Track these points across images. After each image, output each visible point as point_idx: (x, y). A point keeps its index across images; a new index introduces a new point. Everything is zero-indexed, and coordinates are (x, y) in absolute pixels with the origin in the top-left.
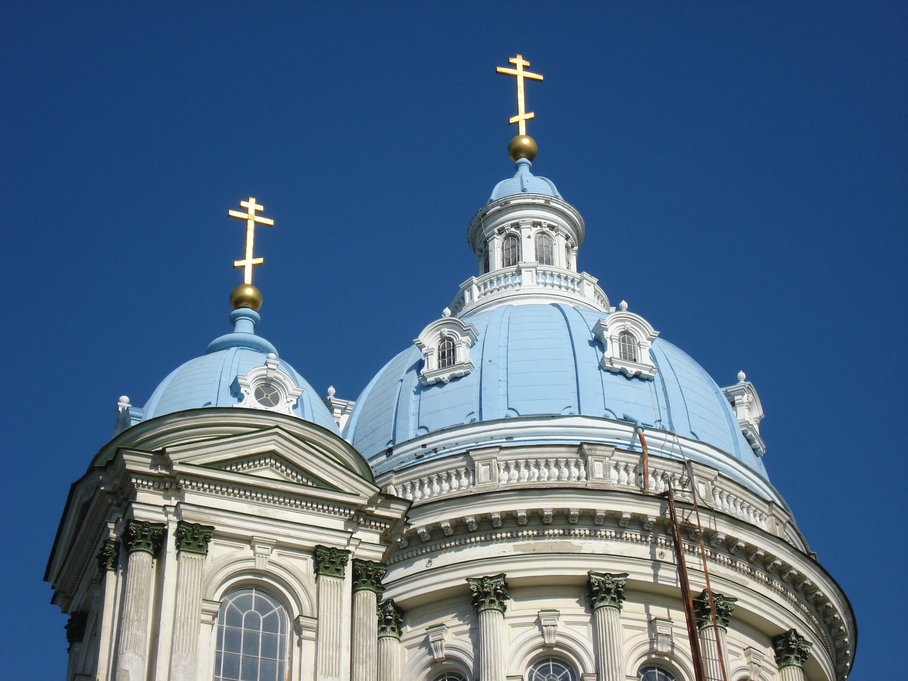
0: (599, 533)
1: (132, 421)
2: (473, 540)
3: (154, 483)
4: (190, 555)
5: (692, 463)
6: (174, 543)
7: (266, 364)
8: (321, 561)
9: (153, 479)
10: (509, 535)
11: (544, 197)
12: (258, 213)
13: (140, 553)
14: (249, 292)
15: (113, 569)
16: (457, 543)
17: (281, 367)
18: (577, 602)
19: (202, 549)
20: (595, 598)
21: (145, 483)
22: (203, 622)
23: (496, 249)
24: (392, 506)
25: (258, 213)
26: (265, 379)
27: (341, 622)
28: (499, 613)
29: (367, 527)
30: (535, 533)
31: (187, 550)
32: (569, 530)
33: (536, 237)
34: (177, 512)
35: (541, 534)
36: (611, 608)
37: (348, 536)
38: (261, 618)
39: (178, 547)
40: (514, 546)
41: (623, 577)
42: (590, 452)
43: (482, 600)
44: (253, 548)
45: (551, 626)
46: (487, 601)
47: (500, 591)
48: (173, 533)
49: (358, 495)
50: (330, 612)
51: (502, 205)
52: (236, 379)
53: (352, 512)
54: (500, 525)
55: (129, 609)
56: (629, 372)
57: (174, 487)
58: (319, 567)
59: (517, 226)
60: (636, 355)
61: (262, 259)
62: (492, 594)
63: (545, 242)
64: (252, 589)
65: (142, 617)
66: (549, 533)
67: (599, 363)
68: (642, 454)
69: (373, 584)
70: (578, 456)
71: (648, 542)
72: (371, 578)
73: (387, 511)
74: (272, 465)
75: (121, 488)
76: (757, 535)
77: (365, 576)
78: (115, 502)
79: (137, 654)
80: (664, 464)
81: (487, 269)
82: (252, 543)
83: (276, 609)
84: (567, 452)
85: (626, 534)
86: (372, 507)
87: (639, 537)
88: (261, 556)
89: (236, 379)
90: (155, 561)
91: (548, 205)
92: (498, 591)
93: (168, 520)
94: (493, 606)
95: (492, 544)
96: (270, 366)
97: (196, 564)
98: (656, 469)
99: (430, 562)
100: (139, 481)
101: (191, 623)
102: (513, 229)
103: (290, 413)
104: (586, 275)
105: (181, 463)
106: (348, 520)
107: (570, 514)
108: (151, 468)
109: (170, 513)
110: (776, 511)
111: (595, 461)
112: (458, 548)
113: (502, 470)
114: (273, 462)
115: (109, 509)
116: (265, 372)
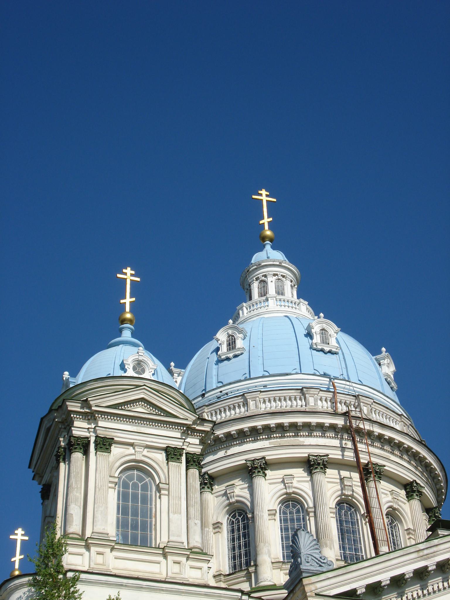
0: (313, 434)
1: (70, 384)
2: (248, 440)
3: (82, 416)
4: (102, 453)
5: (360, 396)
6: (94, 447)
7: (138, 353)
8: (169, 454)
9: (83, 414)
10: (266, 437)
11: (279, 261)
12: (132, 275)
13: (77, 453)
14: (128, 316)
15: (63, 461)
16: (240, 442)
17: (146, 354)
18: (303, 470)
19: (108, 450)
20: (312, 468)
21: (78, 416)
22: (110, 487)
23: (255, 288)
24: (205, 424)
25: (132, 275)
26: (138, 361)
27: (181, 485)
28: (263, 477)
29: (193, 436)
30: (280, 435)
31: (100, 451)
32: (298, 433)
33: (275, 282)
34: (95, 431)
35: (283, 436)
36: (321, 473)
37: (183, 441)
38: (140, 485)
39: (96, 449)
40: (269, 442)
41: (326, 456)
42: (307, 392)
43: (254, 471)
44: (134, 448)
45: (290, 483)
46: (256, 471)
47: (263, 466)
48: (93, 442)
49: (188, 420)
50: (175, 481)
51: (257, 266)
52: (123, 361)
53: (185, 429)
54: (262, 432)
55: (72, 482)
56: (326, 350)
57: (93, 418)
58: (168, 457)
59: (265, 276)
60: (329, 341)
61: (135, 298)
62: (259, 468)
63: (280, 284)
64: (135, 470)
65: (79, 486)
66: (287, 435)
67: (310, 346)
68: (334, 392)
69: (196, 465)
70: (301, 394)
71: (338, 438)
72: (195, 462)
73: (202, 427)
74: (142, 405)
75: (66, 420)
76: (394, 432)
77: (192, 461)
78: (63, 427)
79: (77, 505)
80: (345, 397)
81: (250, 299)
82: (134, 446)
83: (147, 480)
84: (295, 393)
85: (327, 434)
86: (195, 425)
87: (334, 436)
88: (138, 452)
89: (123, 361)
90: (84, 457)
91: (281, 265)
92: (262, 466)
93: (90, 436)
94: (259, 474)
95: (258, 442)
96: (140, 354)
97: (105, 458)
98: (341, 400)
99: (226, 452)
100: (75, 416)
101: (104, 488)
102: (263, 278)
103: (151, 378)
104: (302, 300)
105: (96, 406)
106: (183, 432)
107: (298, 425)
108: (81, 409)
109: (91, 432)
110: (404, 419)
111: (310, 397)
112: (240, 444)
113: (262, 403)
114: (143, 403)
115: (60, 430)
116: (137, 357)
